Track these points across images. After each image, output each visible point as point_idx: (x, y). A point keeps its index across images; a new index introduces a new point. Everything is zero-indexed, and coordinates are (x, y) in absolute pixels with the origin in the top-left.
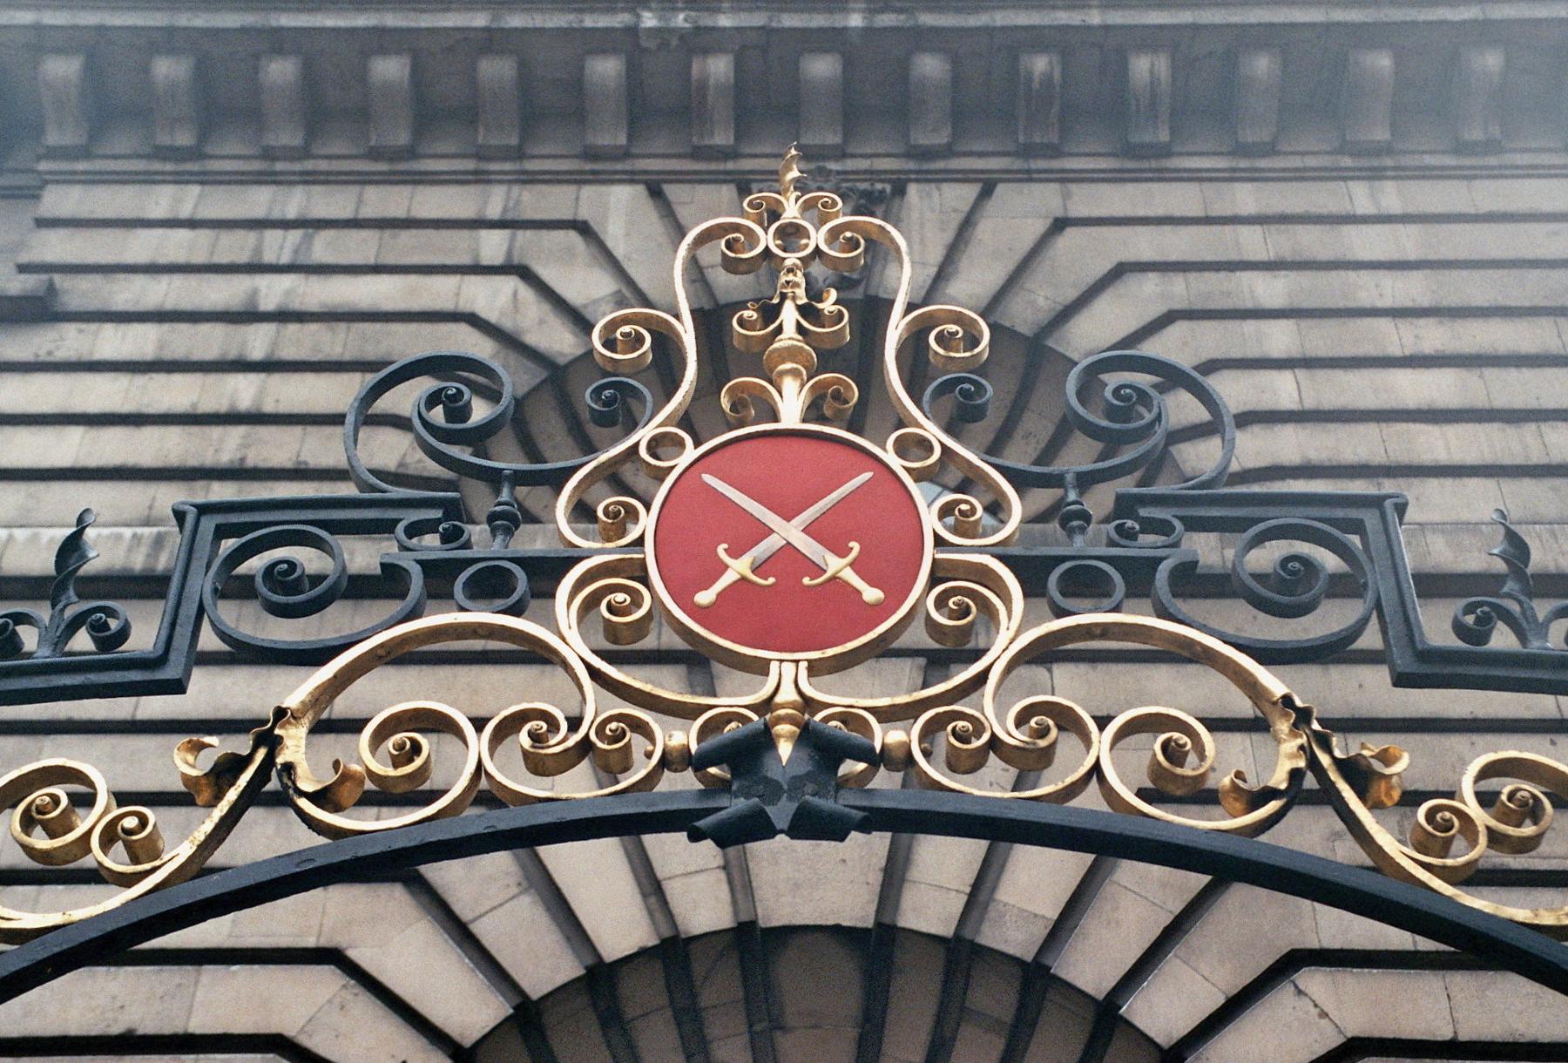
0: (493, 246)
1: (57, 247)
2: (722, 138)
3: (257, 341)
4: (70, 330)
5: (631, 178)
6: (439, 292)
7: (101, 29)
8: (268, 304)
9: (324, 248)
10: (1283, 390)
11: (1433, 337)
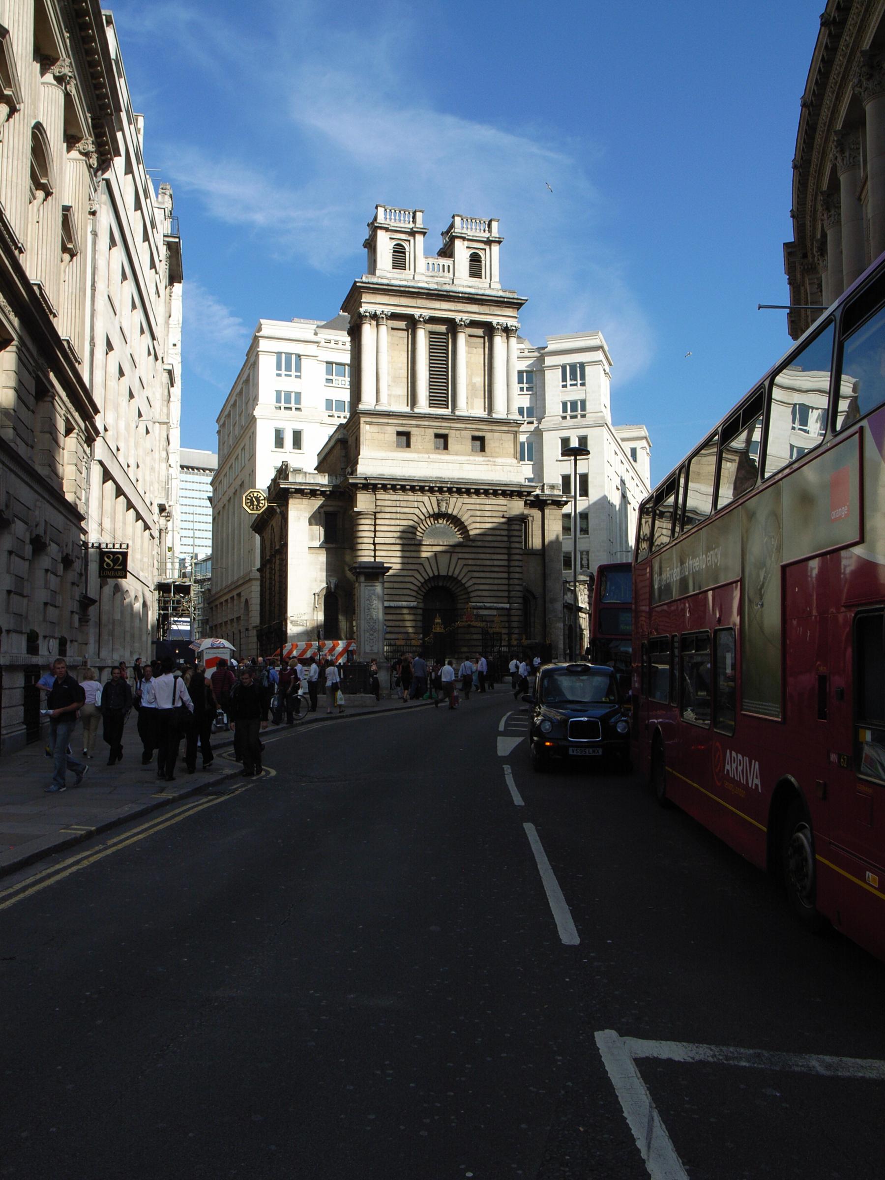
0: (416, 504)
1: (379, 503)
3: (398, 516)
6: (412, 511)
9: (403, 504)
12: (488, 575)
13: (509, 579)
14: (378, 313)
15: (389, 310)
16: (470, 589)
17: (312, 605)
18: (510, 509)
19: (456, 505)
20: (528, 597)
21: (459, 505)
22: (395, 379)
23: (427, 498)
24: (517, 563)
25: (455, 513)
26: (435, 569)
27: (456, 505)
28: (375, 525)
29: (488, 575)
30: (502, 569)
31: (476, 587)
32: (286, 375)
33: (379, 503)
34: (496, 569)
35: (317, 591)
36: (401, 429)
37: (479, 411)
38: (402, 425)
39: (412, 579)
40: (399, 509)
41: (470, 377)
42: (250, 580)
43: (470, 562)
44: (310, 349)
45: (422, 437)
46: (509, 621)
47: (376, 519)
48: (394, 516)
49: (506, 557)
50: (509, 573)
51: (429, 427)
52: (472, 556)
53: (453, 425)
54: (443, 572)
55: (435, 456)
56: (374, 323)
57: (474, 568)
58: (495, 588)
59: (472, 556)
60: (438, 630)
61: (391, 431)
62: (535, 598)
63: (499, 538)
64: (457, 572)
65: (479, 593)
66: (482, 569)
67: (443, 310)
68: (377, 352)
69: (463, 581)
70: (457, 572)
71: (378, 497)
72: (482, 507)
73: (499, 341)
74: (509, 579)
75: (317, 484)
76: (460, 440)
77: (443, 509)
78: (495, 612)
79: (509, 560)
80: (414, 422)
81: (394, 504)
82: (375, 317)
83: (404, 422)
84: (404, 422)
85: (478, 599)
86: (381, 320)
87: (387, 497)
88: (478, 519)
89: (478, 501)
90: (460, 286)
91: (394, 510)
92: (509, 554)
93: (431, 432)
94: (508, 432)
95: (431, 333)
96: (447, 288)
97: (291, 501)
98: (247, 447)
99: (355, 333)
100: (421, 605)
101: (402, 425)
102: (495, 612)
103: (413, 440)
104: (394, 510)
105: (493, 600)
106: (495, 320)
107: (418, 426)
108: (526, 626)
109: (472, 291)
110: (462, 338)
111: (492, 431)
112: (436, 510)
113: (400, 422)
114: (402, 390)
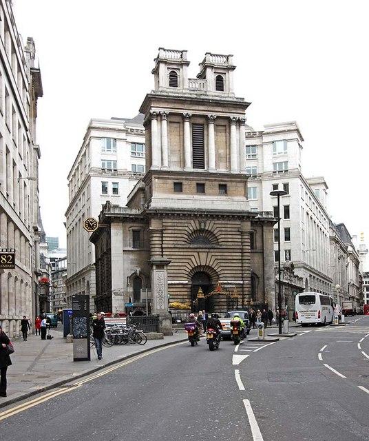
0: (186, 225)
1: (164, 224)
3: (176, 232)
10: (223, 236)
11: (230, 233)
12: (230, 265)
13: (242, 267)
15: (168, 111)
16: (219, 273)
18: (242, 226)
19: (210, 225)
20: (254, 277)
22: (172, 152)
24: (247, 258)
25: (209, 229)
26: (198, 262)
27: (210, 225)
28: (162, 237)
29: (230, 265)
30: (238, 261)
31: (223, 272)
33: (164, 224)
34: (235, 261)
37: (223, 170)
38: (177, 179)
39: (184, 268)
40: (176, 228)
41: (217, 150)
42: (90, 270)
43: (219, 257)
44: (123, 136)
45: (189, 185)
46: (243, 291)
47: (162, 234)
48: (173, 232)
49: (240, 254)
50: (242, 263)
51: (193, 180)
52: (221, 254)
54: (203, 264)
55: (197, 197)
56: (159, 119)
57: (221, 261)
58: (234, 272)
59: (221, 254)
60: (201, 297)
61: (170, 183)
62: (258, 278)
63: (236, 243)
64: (211, 263)
65: (225, 275)
66: (226, 261)
67: (200, 110)
69: (217, 271)
70: (211, 263)
72: (226, 226)
73: (233, 128)
74: (242, 267)
75: (128, 214)
76: (211, 187)
79: (242, 256)
82: (159, 115)
85: (224, 279)
87: (169, 221)
88: (223, 233)
89: (223, 222)
90: (210, 96)
91: (173, 228)
92: (242, 253)
94: (241, 182)
95: (193, 124)
96: (203, 97)
97: (112, 224)
98: (86, 194)
99: (148, 125)
100: (191, 283)
101: (177, 179)
103: (184, 187)
104: (173, 228)
105: (233, 279)
106: (232, 116)
107: (187, 179)
108: (253, 294)
109: (218, 99)
110: (212, 127)
111: (231, 181)
112: (198, 228)
114: (175, 159)
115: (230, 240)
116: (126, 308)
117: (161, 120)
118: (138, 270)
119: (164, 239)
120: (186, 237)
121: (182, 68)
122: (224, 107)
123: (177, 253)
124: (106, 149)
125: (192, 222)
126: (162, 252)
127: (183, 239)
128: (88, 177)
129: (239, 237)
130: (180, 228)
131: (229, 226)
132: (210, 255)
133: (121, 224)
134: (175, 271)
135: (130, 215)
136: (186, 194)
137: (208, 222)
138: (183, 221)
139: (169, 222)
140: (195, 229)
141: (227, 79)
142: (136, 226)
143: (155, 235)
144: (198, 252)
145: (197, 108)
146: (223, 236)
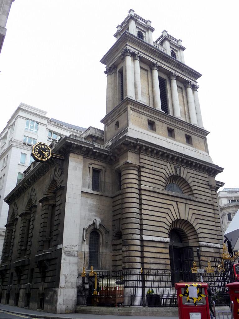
1: (142, 161)
2: (174, 162)
3: (154, 172)
4: (145, 169)
5: (169, 163)
7: (147, 146)
8: (154, 169)
10: (197, 188)
14: (136, 53)
17: (81, 239)
19: (185, 173)
21: (186, 172)
23: (168, 164)
27: (185, 173)
32: (30, 130)
34: (209, 219)
35: (86, 226)
36: (150, 119)
38: (151, 117)
39: (164, 220)
40: (154, 168)
43: (196, 212)
45: (161, 127)
47: (139, 171)
48: (151, 172)
53: (176, 125)
54: (183, 218)
61: (144, 120)
68: (134, 73)
69: (194, 225)
71: (141, 156)
73: (190, 90)
76: (180, 134)
77: (178, 173)
78: (212, 250)
80: (157, 117)
81: (151, 163)
82: (133, 55)
83: (152, 115)
84: (152, 115)
86: (137, 58)
88: (196, 184)
91: (151, 167)
93: (165, 126)
94: (201, 137)
101: (151, 117)
102: (212, 250)
103: (157, 127)
104: (151, 167)
107: (159, 120)
110: (174, 83)
113: (150, 114)
115: (202, 193)
116: (79, 276)
117: (134, 60)
118: (98, 220)
119: (142, 178)
120: (165, 181)
121: (148, 31)
122: (182, 71)
123: (156, 200)
124: (29, 129)
125: (168, 164)
126: (140, 195)
127: (161, 183)
128: (10, 147)
129: (209, 191)
130: (158, 169)
131: (200, 178)
132: (188, 207)
133: (81, 157)
134: (156, 224)
135: (95, 148)
136: (159, 134)
137: (182, 169)
138: (160, 162)
139: (147, 160)
140: (172, 174)
141: (179, 55)
142: (98, 165)
143: (132, 172)
144: (177, 202)
145: (163, 62)
146: (197, 188)
